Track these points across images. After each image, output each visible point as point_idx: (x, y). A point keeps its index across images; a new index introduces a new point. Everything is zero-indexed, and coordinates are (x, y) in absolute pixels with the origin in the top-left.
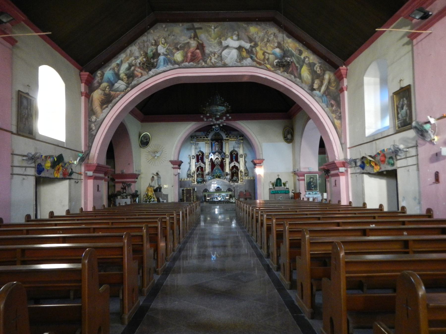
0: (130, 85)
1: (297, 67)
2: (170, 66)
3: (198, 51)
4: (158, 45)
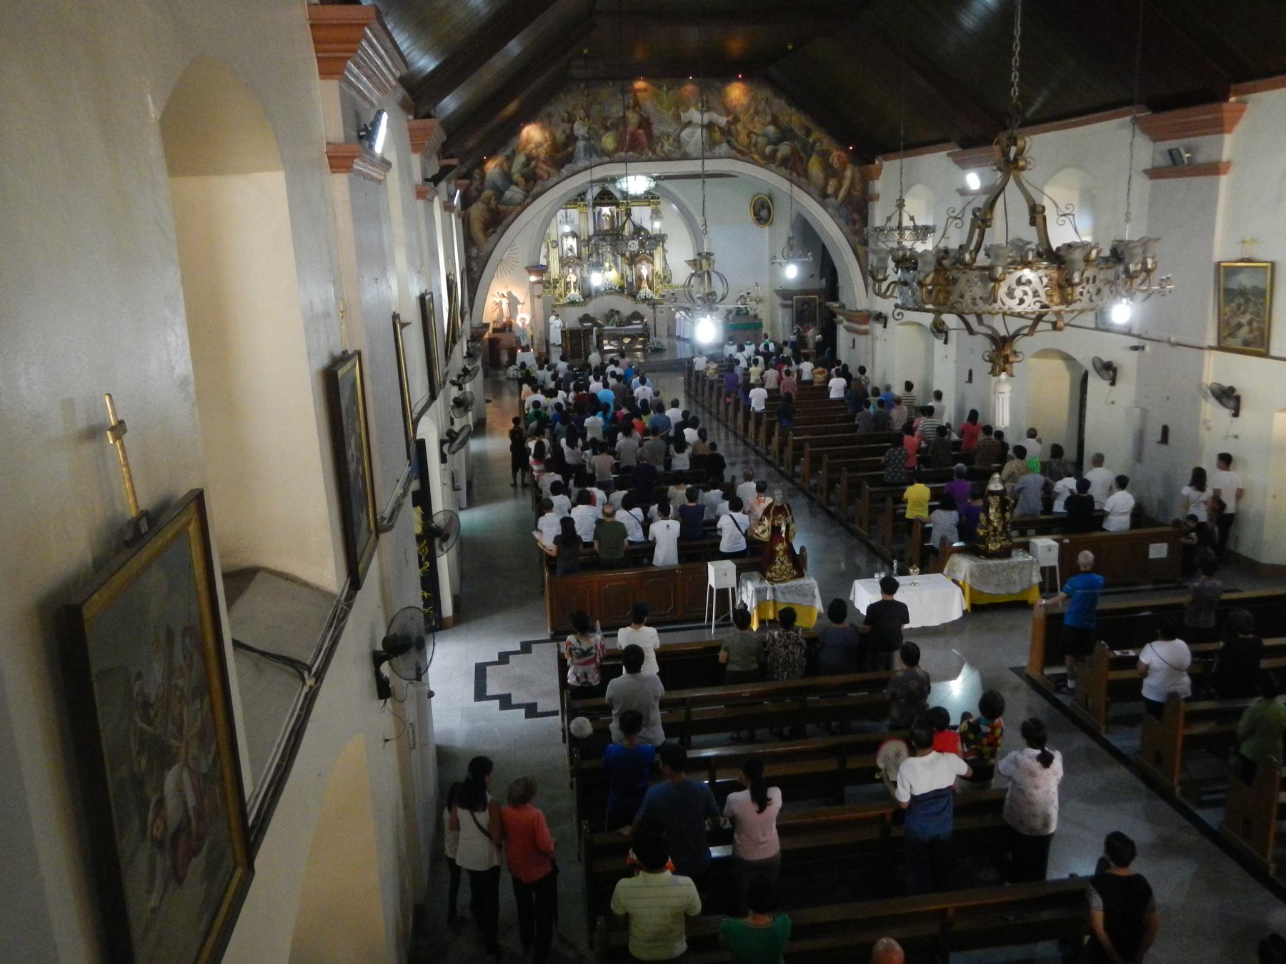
0: (531, 193)
1: (801, 158)
2: (595, 159)
3: (641, 131)
4: (574, 123)
